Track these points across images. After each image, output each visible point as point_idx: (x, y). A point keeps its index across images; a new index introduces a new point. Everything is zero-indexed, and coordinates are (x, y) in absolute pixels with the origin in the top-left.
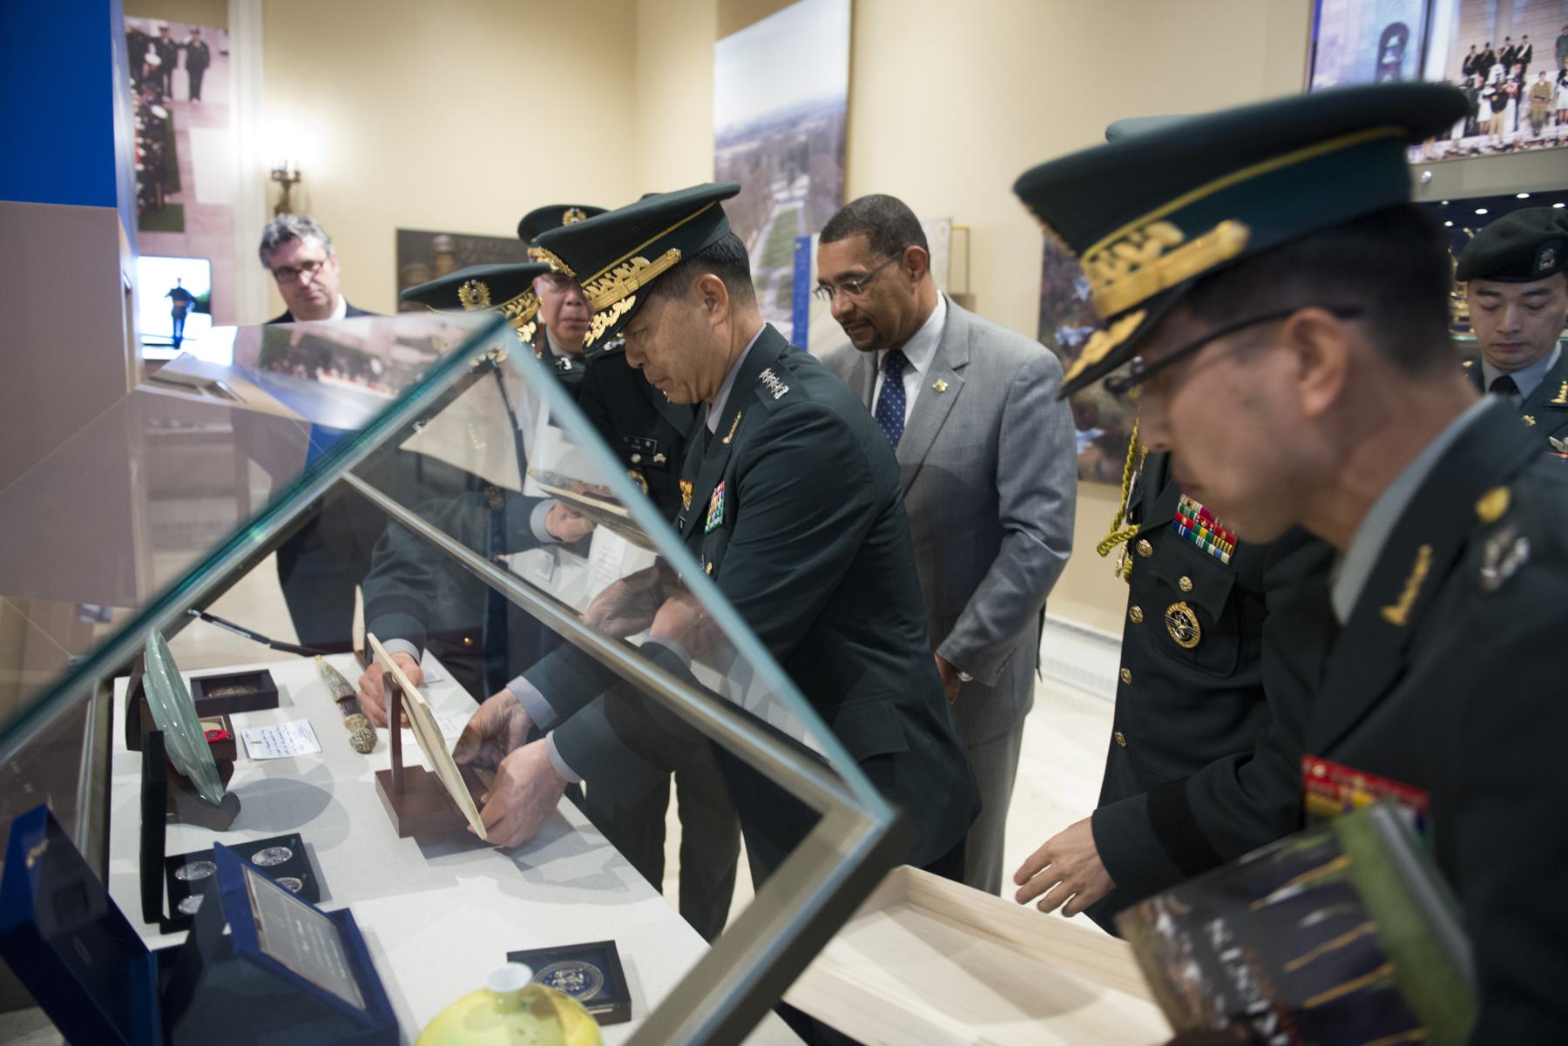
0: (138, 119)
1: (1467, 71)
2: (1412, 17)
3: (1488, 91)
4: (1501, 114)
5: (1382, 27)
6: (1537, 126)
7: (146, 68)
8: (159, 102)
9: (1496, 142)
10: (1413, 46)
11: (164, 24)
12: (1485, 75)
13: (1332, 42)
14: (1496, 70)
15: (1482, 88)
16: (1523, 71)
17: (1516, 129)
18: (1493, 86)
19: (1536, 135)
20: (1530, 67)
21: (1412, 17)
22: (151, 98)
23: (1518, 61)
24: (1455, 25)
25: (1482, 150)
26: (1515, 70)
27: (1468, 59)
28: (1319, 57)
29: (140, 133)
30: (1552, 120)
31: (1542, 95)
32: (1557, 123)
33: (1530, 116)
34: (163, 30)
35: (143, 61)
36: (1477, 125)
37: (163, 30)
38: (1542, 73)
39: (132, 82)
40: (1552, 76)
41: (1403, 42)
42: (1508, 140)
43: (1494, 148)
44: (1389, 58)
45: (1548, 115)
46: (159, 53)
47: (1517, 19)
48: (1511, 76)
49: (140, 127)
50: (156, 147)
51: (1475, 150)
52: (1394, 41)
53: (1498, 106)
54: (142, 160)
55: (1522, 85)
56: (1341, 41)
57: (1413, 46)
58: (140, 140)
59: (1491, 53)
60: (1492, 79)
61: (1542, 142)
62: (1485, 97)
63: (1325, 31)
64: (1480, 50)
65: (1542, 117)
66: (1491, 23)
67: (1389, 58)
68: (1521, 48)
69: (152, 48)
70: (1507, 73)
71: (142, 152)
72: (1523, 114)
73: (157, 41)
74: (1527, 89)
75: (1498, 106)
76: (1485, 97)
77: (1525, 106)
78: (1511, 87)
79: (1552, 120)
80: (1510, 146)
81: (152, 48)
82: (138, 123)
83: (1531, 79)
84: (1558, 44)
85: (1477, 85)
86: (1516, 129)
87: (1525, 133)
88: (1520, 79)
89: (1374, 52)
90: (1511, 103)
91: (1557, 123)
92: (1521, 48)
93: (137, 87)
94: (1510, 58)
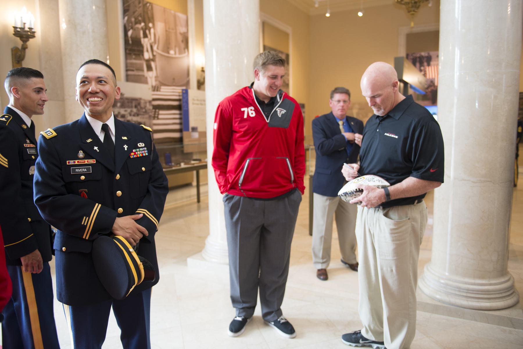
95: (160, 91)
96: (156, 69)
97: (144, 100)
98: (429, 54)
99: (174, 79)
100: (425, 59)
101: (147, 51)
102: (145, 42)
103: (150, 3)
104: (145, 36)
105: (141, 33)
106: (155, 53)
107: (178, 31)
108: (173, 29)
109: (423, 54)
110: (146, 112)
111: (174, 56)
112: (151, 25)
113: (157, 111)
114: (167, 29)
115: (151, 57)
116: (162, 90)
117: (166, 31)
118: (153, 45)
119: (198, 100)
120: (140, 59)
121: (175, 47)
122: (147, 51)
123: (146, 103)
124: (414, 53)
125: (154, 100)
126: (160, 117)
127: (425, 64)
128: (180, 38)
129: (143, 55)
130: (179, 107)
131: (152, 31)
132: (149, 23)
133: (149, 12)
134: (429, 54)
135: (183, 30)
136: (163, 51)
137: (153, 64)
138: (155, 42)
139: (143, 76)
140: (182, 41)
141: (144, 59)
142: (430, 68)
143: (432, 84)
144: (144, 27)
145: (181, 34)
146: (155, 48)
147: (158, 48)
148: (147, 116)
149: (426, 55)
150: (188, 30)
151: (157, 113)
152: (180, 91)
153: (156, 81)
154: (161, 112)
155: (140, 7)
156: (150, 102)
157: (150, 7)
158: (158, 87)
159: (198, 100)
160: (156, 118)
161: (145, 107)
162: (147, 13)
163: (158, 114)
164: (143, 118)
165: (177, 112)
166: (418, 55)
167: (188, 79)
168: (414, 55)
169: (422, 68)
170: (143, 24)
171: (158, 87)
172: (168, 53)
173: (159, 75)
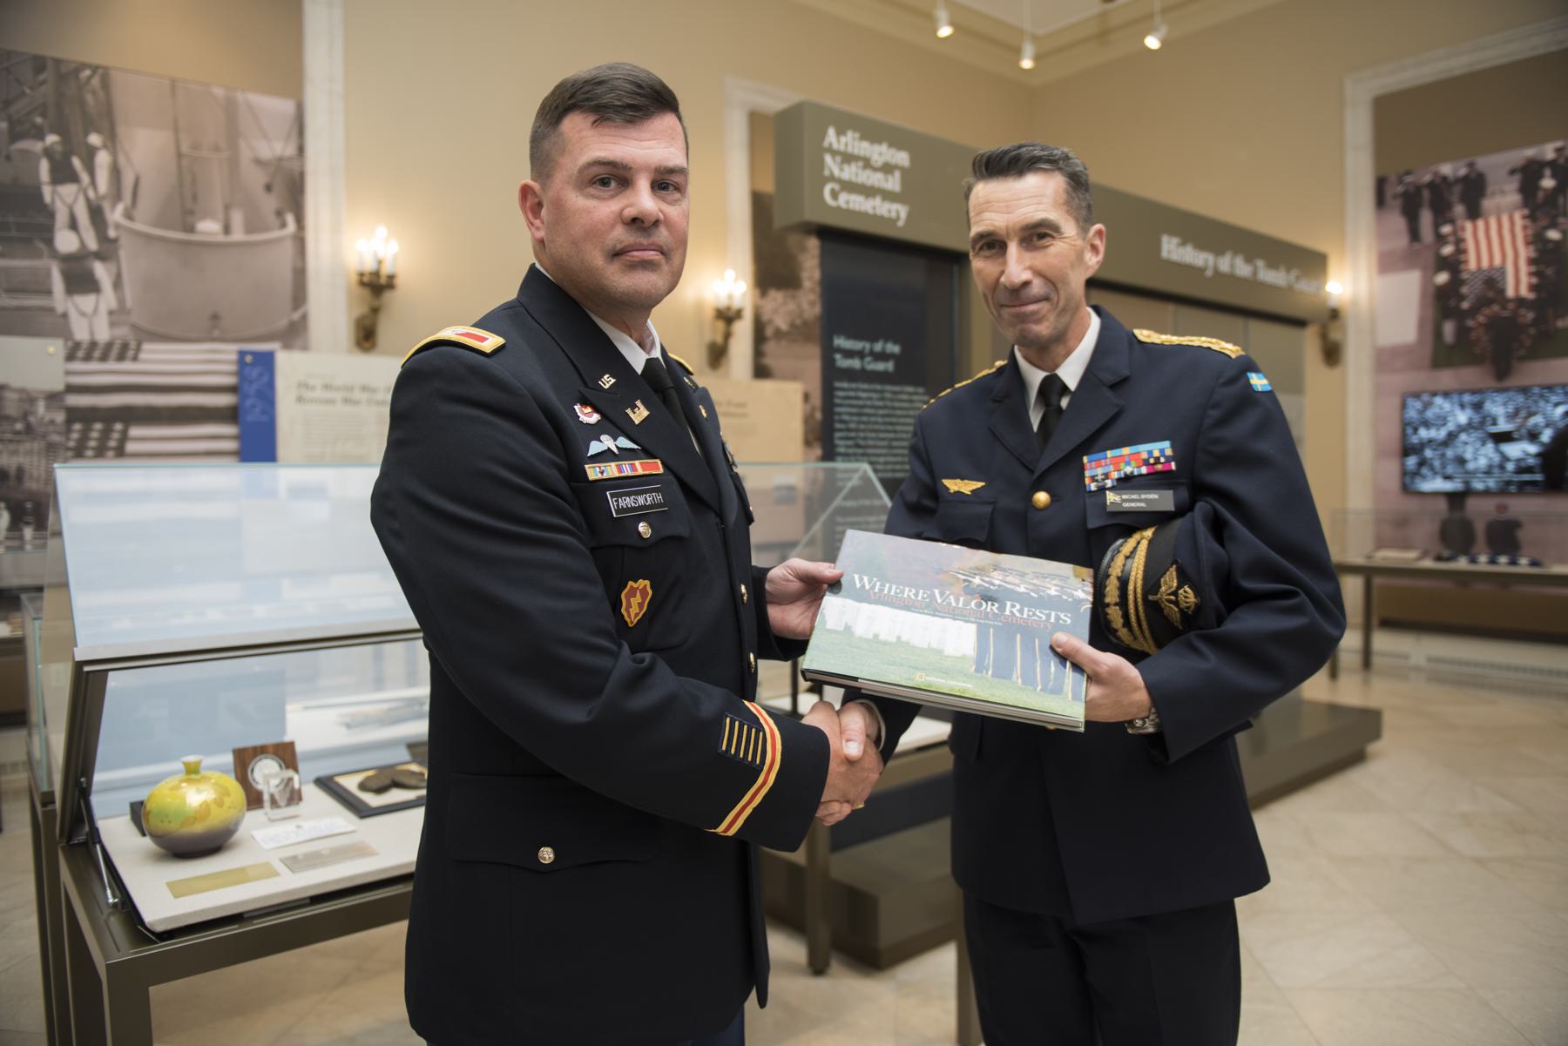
0: (1532, 248)
7: (1541, 195)
8: (1553, 225)
11: (1559, 144)
22: (1544, 222)
29: (1531, 262)
34: (1559, 150)
35: (1537, 187)
37: (1559, 150)
39: (1526, 212)
46: (1554, 176)
49: (1533, 255)
50: (1549, 272)
54: (1532, 288)
58: (1533, 269)
69: (1548, 172)
71: (1534, 280)
73: (1552, 164)
81: (1548, 172)
82: (1524, 253)
93: (1532, 217)
95: (135, 359)
96: (117, 284)
97: (22, 391)
98: (1471, 165)
99: (215, 317)
100: (1458, 189)
101: (73, 225)
102: (64, 199)
103: (95, 69)
104: (63, 174)
105: (44, 167)
106: (112, 233)
107: (245, 154)
108: (217, 149)
109: (1446, 169)
110: (29, 430)
111: (221, 238)
112: (94, 139)
113: (118, 426)
114: (185, 148)
115: (93, 245)
116: (142, 356)
117: (179, 156)
118: (106, 206)
119: (327, 387)
120: (39, 256)
121: (227, 208)
122: (73, 225)
123: (29, 398)
124: (1408, 173)
125: (72, 389)
126: (131, 447)
127: (1459, 210)
128: (255, 179)
129: (49, 241)
130: (230, 415)
131: (103, 159)
132: (86, 134)
133: (89, 98)
134: (1471, 165)
135: (278, 148)
136: (158, 223)
137: (101, 271)
138: (117, 196)
139: (51, 310)
140: (268, 188)
141: (54, 254)
142: (1480, 223)
143: (1491, 294)
144: (59, 148)
145: (259, 162)
146: (115, 215)
147: (129, 215)
148: (37, 445)
149: (1463, 172)
150: (301, 150)
151: (116, 435)
152: (234, 357)
153: (112, 325)
154: (135, 431)
155: (44, 82)
156: (53, 398)
157: (96, 82)
158: (125, 347)
159: (327, 387)
160: (111, 453)
161: (25, 416)
162: (82, 103)
163: (124, 438)
164: (14, 453)
165: (229, 430)
166: (1427, 178)
167: (296, 316)
168: (1409, 179)
169: (1446, 229)
170: (52, 139)
171: (125, 347)
172: (191, 229)
173: (129, 303)
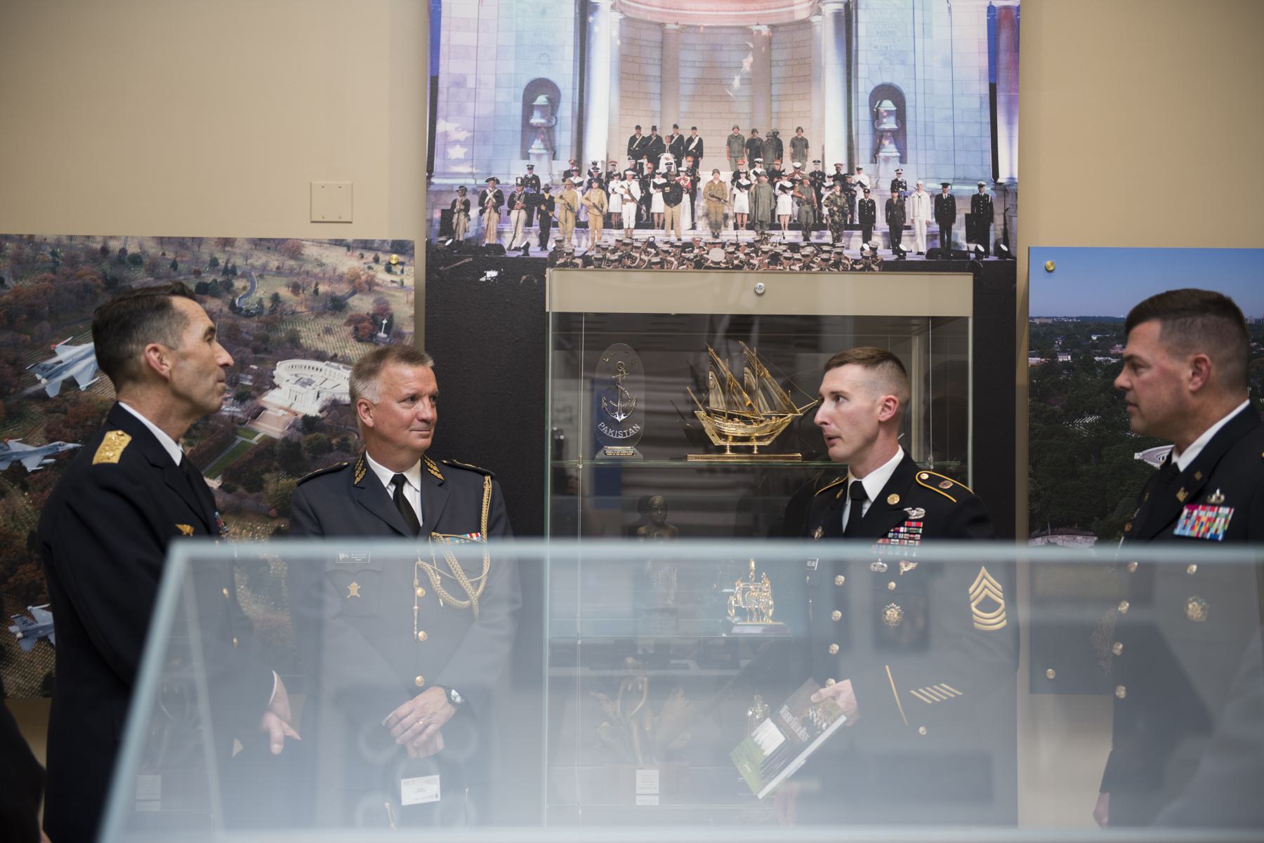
1: (634, 154)
2: (563, 75)
3: (659, 180)
4: (675, 209)
5: (525, 81)
6: (715, 227)
9: (673, 239)
10: (566, 111)
12: (655, 162)
13: (459, 83)
14: (666, 158)
15: (653, 176)
16: (696, 165)
17: (694, 227)
18: (664, 176)
19: (717, 237)
20: (702, 162)
21: (563, 75)
23: (689, 154)
24: (616, 99)
25: (660, 245)
26: (686, 163)
27: (633, 139)
28: (442, 98)
30: (731, 223)
31: (717, 196)
32: (736, 227)
33: (707, 215)
36: (650, 216)
38: (716, 172)
40: (726, 176)
41: (554, 103)
42: (687, 237)
43: (672, 245)
44: (537, 119)
45: (726, 217)
47: (684, 106)
48: (683, 168)
51: (652, 244)
52: (541, 100)
53: (672, 199)
55: (695, 180)
56: (471, 83)
57: (566, 111)
59: (659, 139)
60: (663, 168)
61: (723, 245)
62: (656, 186)
63: (448, 68)
64: (646, 132)
65: (720, 218)
66: (656, 105)
67: (537, 119)
68: (691, 140)
70: (679, 164)
72: (699, 212)
74: (701, 185)
75: (672, 199)
76: (656, 186)
77: (701, 204)
78: (685, 181)
79: (731, 223)
80: (688, 246)
83: (705, 176)
84: (729, 143)
85: (646, 172)
86: (694, 227)
87: (704, 232)
88: (693, 170)
89: (517, 109)
90: (686, 198)
91: (736, 227)
92: (691, 140)
94: (681, 148)
